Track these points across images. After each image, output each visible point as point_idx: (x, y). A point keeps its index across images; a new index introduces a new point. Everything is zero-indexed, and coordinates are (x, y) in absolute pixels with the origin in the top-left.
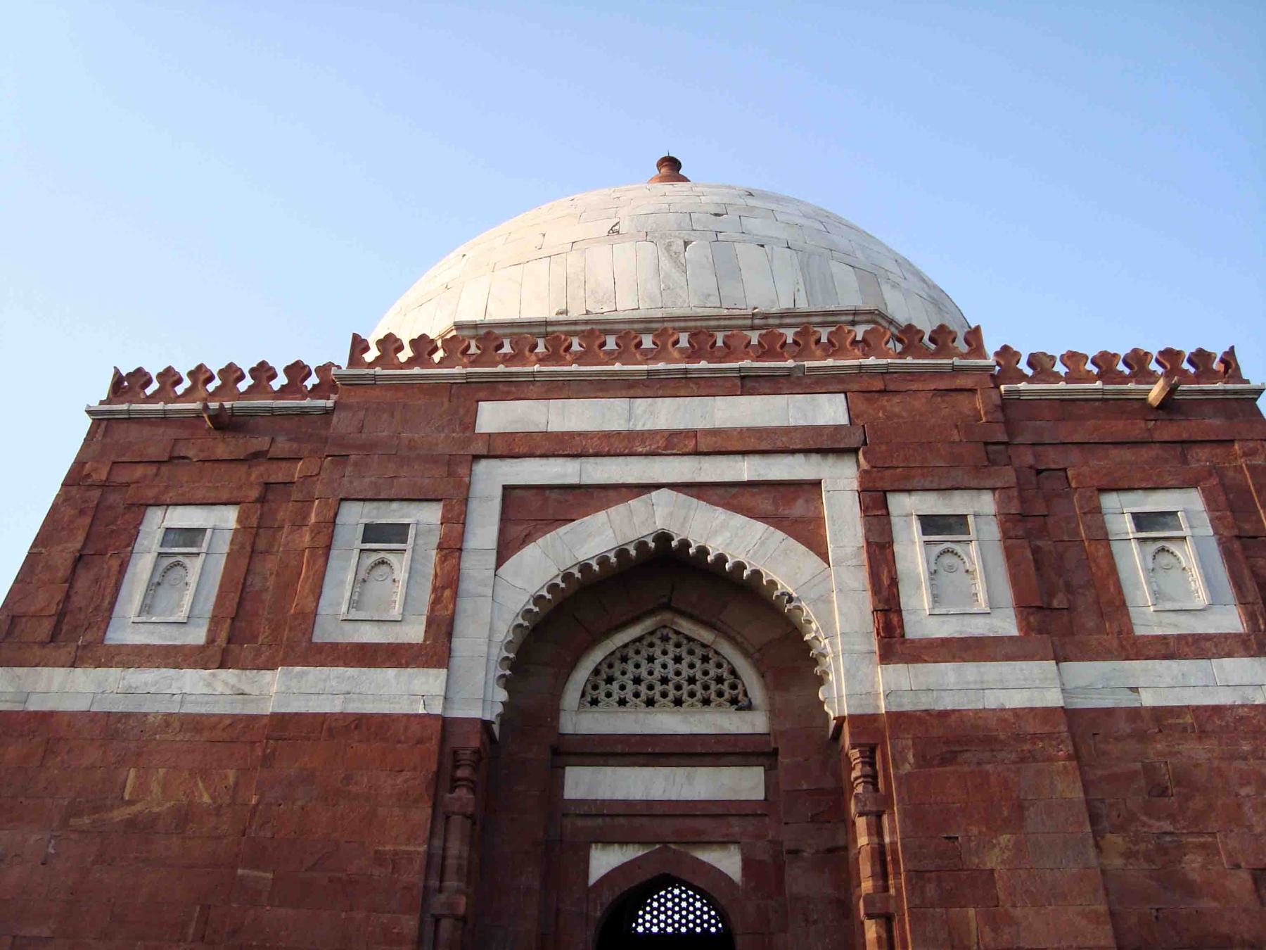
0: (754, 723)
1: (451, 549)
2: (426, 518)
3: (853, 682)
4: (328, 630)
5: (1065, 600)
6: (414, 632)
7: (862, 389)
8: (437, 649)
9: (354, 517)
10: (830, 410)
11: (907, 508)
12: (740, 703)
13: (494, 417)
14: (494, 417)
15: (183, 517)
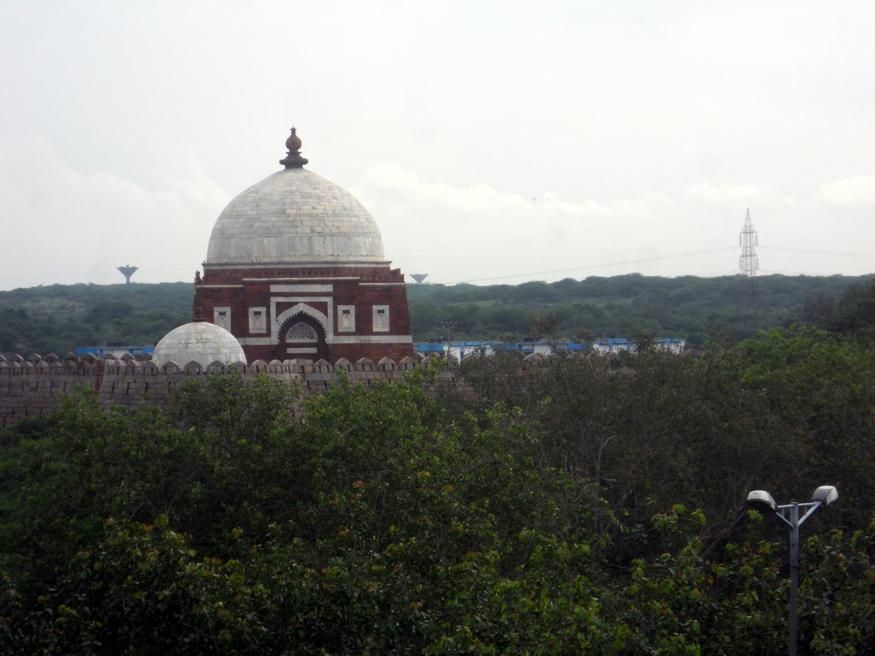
0: (315, 341)
1: (268, 314)
2: (263, 310)
3: (330, 339)
4: (251, 331)
5: (364, 325)
6: (264, 331)
7: (335, 283)
8: (268, 334)
9: (252, 310)
10: (329, 288)
11: (341, 308)
12: (312, 338)
13: (274, 289)
14: (274, 289)
15: (222, 309)
